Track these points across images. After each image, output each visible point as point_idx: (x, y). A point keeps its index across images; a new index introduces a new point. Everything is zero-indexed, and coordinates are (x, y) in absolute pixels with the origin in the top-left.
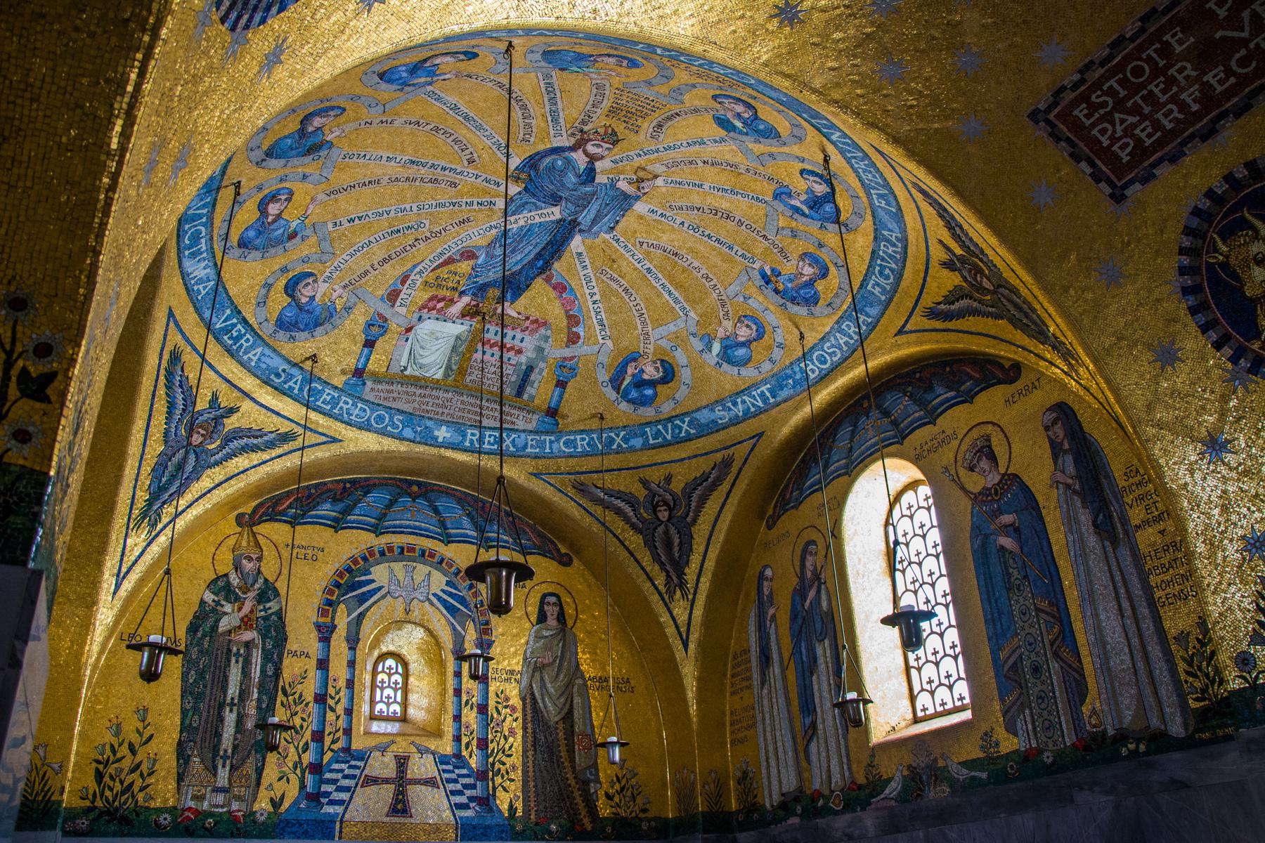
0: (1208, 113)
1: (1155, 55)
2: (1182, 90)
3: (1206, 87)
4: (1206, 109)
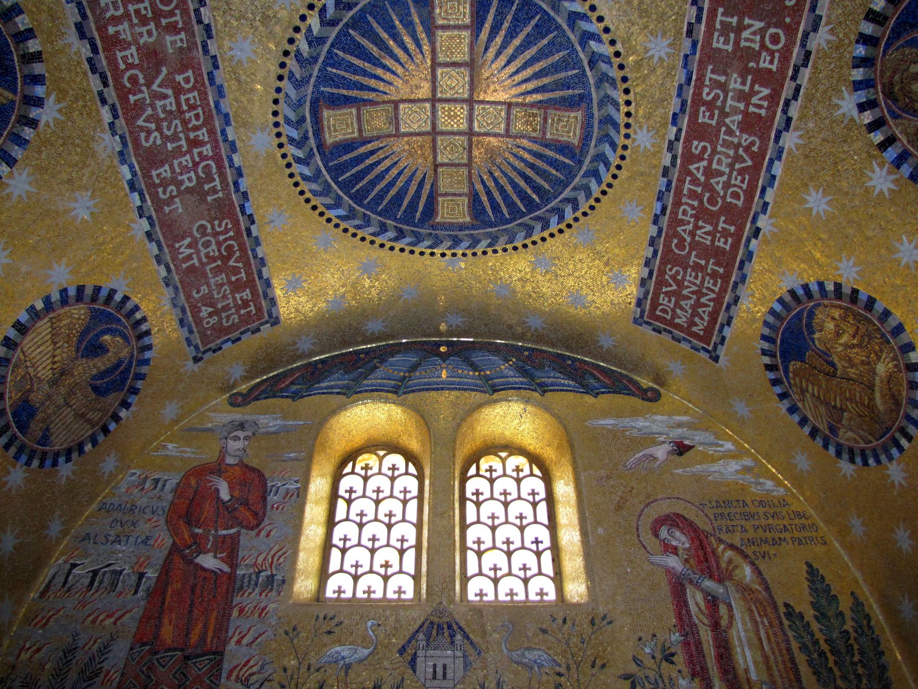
0: (101, 37)
1: (173, 19)
2: (132, 26)
3: (125, 45)
4: (105, 38)
